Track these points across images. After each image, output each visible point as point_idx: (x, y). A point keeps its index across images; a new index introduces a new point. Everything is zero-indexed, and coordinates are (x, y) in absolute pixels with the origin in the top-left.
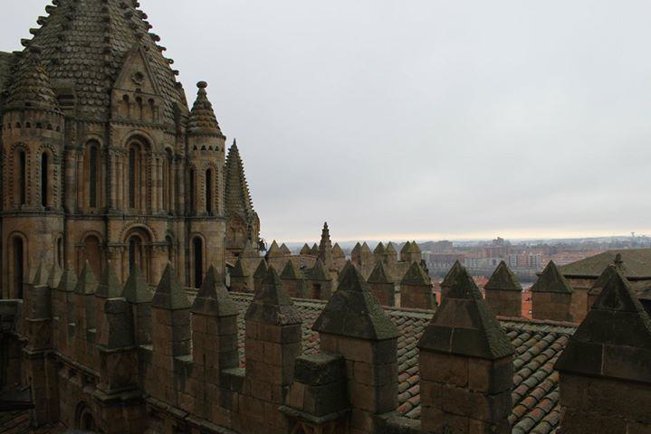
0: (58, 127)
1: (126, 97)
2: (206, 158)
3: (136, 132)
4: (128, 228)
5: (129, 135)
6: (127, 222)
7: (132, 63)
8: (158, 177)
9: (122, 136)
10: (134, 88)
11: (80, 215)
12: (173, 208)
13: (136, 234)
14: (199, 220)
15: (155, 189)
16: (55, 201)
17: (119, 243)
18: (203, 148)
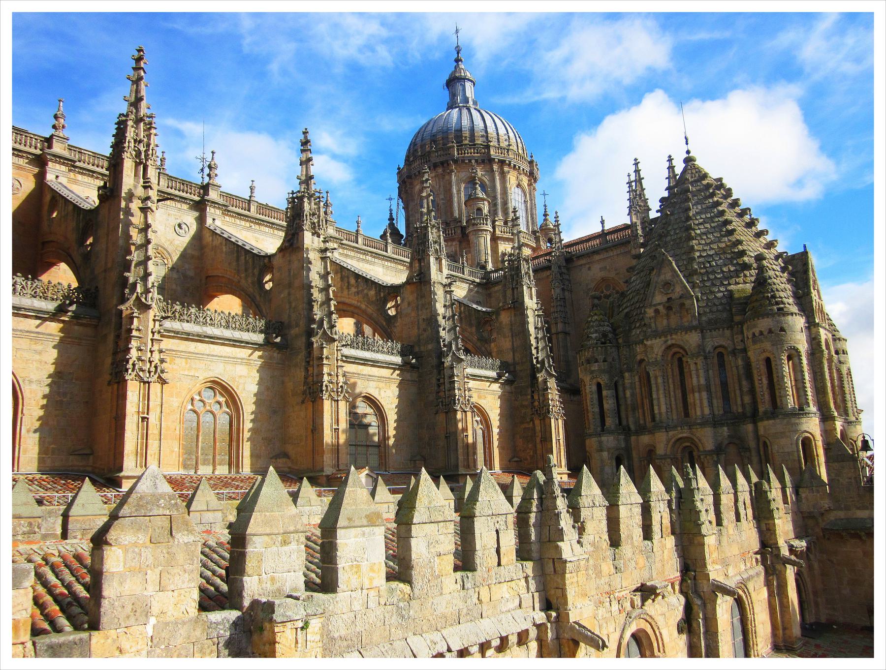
0: (605, 358)
1: (657, 311)
2: (757, 346)
3: (669, 343)
4: (673, 440)
5: (663, 348)
6: (671, 433)
7: (659, 275)
8: (699, 381)
9: (656, 350)
10: (665, 299)
11: (642, 430)
12: (740, 410)
13: (688, 444)
14: (762, 420)
15: (697, 395)
16: (610, 422)
17: (665, 455)
18: (754, 334)
